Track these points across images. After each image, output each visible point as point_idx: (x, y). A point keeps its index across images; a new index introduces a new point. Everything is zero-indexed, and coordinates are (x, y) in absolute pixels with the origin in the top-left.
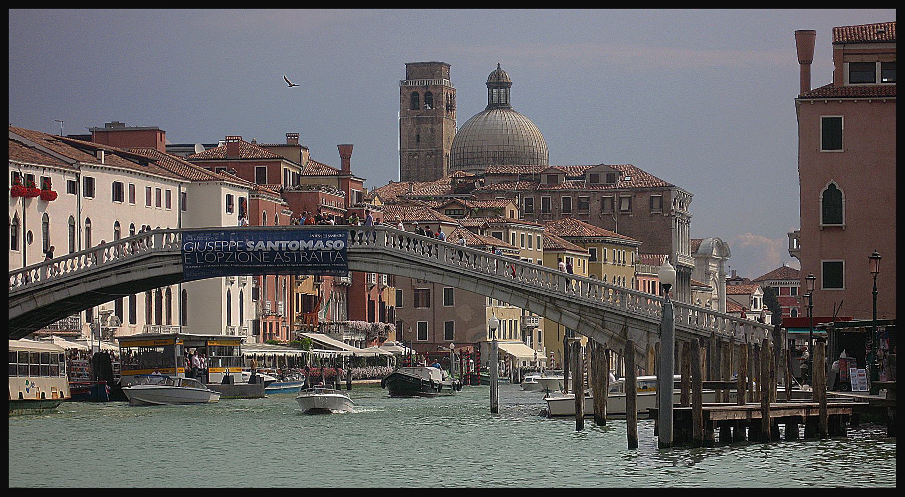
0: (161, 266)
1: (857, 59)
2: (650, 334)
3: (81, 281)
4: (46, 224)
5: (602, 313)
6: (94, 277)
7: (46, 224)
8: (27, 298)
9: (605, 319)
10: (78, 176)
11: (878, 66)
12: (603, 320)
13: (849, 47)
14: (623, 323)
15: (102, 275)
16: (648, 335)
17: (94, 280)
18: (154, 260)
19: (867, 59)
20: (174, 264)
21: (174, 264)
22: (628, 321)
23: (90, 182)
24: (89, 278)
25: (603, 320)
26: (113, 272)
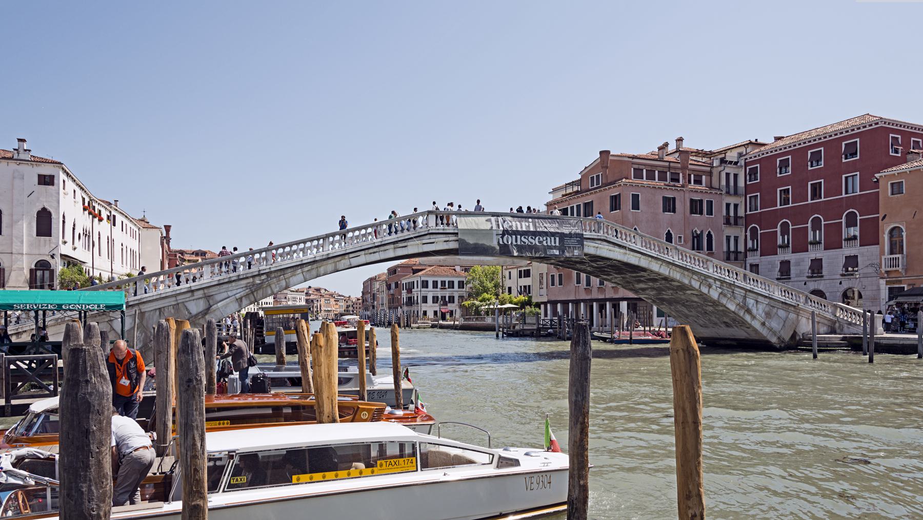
0: (433, 243)
3: (363, 252)
4: (99, 238)
5: (733, 288)
6: (375, 250)
7: (99, 238)
10: (110, 212)
12: (733, 292)
13: (635, 160)
15: (382, 248)
16: (757, 303)
17: (374, 253)
18: (428, 237)
19: (641, 167)
20: (445, 241)
21: (445, 241)
22: (748, 293)
23: (114, 216)
24: (371, 251)
26: (392, 246)
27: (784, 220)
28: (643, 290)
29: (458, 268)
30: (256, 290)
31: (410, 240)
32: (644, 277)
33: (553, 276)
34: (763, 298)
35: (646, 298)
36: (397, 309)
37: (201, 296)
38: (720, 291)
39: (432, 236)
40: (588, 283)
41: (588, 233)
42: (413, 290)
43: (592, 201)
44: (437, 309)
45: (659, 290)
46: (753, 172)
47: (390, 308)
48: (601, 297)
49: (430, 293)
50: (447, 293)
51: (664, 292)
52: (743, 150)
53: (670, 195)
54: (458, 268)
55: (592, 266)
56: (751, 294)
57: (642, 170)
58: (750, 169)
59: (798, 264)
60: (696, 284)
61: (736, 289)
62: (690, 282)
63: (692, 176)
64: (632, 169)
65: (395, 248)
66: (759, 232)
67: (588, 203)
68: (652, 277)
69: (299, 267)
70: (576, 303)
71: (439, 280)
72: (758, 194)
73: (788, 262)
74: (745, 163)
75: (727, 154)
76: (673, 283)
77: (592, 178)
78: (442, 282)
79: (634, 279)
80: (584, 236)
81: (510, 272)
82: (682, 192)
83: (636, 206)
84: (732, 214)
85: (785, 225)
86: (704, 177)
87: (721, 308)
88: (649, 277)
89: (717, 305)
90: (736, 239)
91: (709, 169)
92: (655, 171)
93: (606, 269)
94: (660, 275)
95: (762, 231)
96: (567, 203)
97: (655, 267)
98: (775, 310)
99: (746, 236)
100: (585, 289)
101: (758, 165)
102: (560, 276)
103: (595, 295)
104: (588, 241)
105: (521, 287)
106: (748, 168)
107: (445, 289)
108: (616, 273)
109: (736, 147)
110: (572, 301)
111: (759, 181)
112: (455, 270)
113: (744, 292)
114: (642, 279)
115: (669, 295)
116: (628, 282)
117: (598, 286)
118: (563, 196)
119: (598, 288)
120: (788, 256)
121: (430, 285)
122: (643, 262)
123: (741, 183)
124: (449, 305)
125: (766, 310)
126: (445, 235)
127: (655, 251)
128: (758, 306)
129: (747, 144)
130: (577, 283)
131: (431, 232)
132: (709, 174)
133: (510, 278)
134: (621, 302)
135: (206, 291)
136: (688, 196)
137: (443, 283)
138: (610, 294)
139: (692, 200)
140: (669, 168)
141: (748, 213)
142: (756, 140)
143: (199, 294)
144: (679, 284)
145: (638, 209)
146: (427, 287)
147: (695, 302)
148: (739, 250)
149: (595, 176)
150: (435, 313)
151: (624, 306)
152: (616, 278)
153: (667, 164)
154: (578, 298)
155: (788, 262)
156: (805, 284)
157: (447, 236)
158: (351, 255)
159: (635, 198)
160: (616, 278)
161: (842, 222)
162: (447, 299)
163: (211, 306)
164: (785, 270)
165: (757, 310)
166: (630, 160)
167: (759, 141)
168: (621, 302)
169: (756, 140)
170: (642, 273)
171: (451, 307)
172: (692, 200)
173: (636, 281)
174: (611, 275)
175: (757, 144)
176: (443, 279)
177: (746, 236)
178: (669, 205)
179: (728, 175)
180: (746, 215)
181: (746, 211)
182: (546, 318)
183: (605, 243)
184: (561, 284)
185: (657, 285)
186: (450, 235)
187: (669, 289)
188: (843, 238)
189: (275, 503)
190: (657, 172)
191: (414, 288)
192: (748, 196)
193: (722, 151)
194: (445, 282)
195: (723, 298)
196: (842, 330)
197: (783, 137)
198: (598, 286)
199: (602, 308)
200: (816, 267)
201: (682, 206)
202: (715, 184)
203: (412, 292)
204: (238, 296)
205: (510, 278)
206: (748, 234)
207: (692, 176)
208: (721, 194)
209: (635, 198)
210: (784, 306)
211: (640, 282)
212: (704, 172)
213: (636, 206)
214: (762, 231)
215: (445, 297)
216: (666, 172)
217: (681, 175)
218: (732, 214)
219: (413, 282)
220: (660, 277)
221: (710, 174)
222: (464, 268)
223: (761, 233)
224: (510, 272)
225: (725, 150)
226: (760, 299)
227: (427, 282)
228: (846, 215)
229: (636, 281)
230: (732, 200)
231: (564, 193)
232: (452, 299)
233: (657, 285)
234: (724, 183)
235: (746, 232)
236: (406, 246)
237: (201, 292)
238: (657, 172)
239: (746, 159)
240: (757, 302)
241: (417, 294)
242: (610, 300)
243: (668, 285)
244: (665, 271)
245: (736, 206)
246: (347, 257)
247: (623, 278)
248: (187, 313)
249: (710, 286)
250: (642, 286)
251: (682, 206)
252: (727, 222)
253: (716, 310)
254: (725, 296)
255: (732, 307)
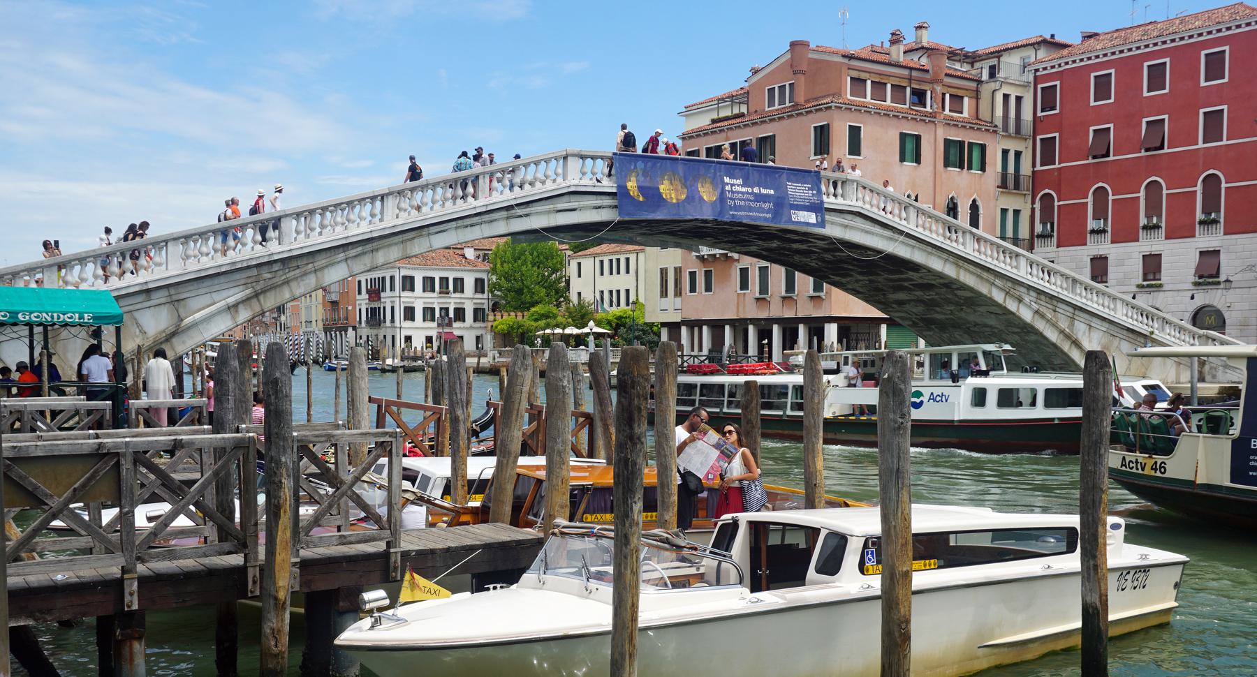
1: (855, 74)
2: (1092, 329)
3: (453, 224)
8: (360, 249)
9: (1057, 309)
11: (869, 83)
14: (1071, 315)
15: (487, 218)
16: (1090, 329)
18: (566, 198)
19: (863, 76)
22: (1077, 312)
24: (468, 222)
25: (1055, 311)
26: (504, 214)
27: (1100, 184)
28: (901, 303)
29: (470, 253)
30: (264, 292)
31: (534, 204)
32: (912, 280)
33: (693, 274)
34: (1099, 322)
35: (902, 318)
36: (346, 331)
37: (163, 300)
38: (1035, 306)
39: (573, 198)
40: (790, 286)
41: (832, 199)
42: (383, 295)
43: (774, 136)
44: (434, 334)
45: (931, 304)
46: (1049, 93)
47: (327, 330)
48: (789, 314)
49: (419, 299)
50: (452, 302)
51: (938, 309)
52: (1030, 54)
53: (911, 130)
54: (470, 253)
55: (823, 260)
56: (1082, 314)
57: (865, 81)
58: (1042, 88)
59: (1121, 263)
60: (998, 296)
61: (1060, 305)
62: (990, 291)
63: (947, 96)
64: (849, 79)
65: (508, 218)
66: (1056, 204)
67: (765, 138)
68: (925, 281)
69: (341, 249)
70: (739, 326)
71: (437, 276)
72: (1057, 135)
73: (1158, 257)
74: (1035, 77)
75: (1002, 59)
76: (960, 293)
77: (771, 91)
78: (441, 279)
79: (891, 284)
80: (826, 206)
81: (579, 264)
82: (932, 126)
83: (855, 148)
84: (1011, 169)
85: (1101, 194)
86: (966, 100)
87: (1034, 338)
88: (920, 281)
89: (1029, 332)
90: (1017, 212)
91: (974, 85)
92: (885, 84)
93: (846, 266)
94: (941, 278)
95: (1061, 203)
96: (723, 135)
97: (936, 264)
98: (1116, 342)
99: (1033, 210)
100: (758, 299)
101: (1058, 83)
102: (708, 274)
103: (777, 310)
104: (833, 213)
105: (602, 292)
106: (1040, 86)
107: (448, 293)
108: (860, 273)
109: (1018, 47)
110: (732, 322)
111: (1057, 111)
112: (463, 256)
113: (1071, 310)
114: (906, 284)
115: (945, 314)
116: (878, 290)
117: (783, 294)
118: (714, 121)
119: (784, 298)
120: (1103, 247)
121: (418, 284)
122: (918, 256)
123: (1027, 115)
124: (455, 325)
125: (1103, 341)
126: (595, 197)
127: (938, 235)
128: (1092, 334)
129: (1038, 43)
130: (741, 289)
131: (573, 189)
132: (974, 94)
133: (580, 276)
134: (827, 326)
135: (172, 291)
136: (942, 133)
137: (444, 281)
138: (805, 309)
139: (948, 143)
140: (910, 79)
141: (1038, 168)
142: (1053, 36)
143: (159, 297)
144: (973, 295)
145: (859, 155)
146: (412, 289)
147: (991, 326)
148: (1021, 236)
149: (776, 87)
150: (429, 340)
151: (831, 331)
152: (857, 281)
153: (906, 72)
154: (742, 316)
155: (1158, 257)
156: (1134, 298)
157: (599, 197)
158: (433, 229)
159: (855, 132)
160: (857, 281)
161: (1195, 191)
162: (451, 314)
163: (182, 320)
164: (1099, 268)
165: (1090, 341)
166: (846, 61)
167: (1058, 39)
168: (827, 326)
169: (1053, 36)
170: (911, 274)
171: (457, 329)
172: (948, 143)
173: (893, 287)
174: (851, 276)
175: (1052, 44)
176: (444, 274)
177: (1033, 210)
178: (911, 149)
179: (1006, 97)
180: (1034, 172)
181: (1034, 165)
182: (701, 353)
183: (859, 220)
184: (708, 288)
185: (931, 295)
186: (603, 197)
187: (949, 302)
188: (1197, 220)
189: (762, 617)
190: (889, 86)
191: (384, 290)
192: (1039, 137)
193: (994, 52)
194: (432, 279)
195: (1040, 320)
196: (1214, 377)
197: (1096, 34)
198: (783, 294)
199: (765, 334)
200: (1152, 265)
201: (932, 149)
202: (985, 114)
203: (379, 299)
204: (231, 300)
205: (580, 276)
206: (1037, 206)
207: (947, 96)
208: (995, 132)
209: (855, 132)
210: (1131, 335)
211: (901, 289)
212: (967, 90)
213: (855, 148)
214: (1061, 203)
215: (447, 310)
216: (905, 87)
217: (929, 93)
218: (1011, 169)
219: (384, 278)
220: (941, 281)
221: (976, 96)
222: (481, 253)
223: (1059, 206)
224: (579, 264)
225: (998, 52)
226: (1096, 323)
227: (412, 279)
228: (1204, 180)
229: (893, 287)
230: (1013, 146)
231: (715, 116)
232: (460, 314)
233: (931, 295)
234: (999, 112)
235: (1033, 202)
236: (527, 215)
237: (164, 293)
238: (889, 86)
239: (1037, 70)
240: (1090, 326)
241: (393, 302)
242: (805, 320)
243: (950, 296)
244: (950, 271)
245: (1018, 154)
246: (425, 232)
247: (870, 281)
248: (138, 330)
249: (1020, 300)
250: (902, 296)
251: (932, 149)
252: (1003, 185)
253: (1024, 340)
254: (1043, 316)
255: (1052, 335)
